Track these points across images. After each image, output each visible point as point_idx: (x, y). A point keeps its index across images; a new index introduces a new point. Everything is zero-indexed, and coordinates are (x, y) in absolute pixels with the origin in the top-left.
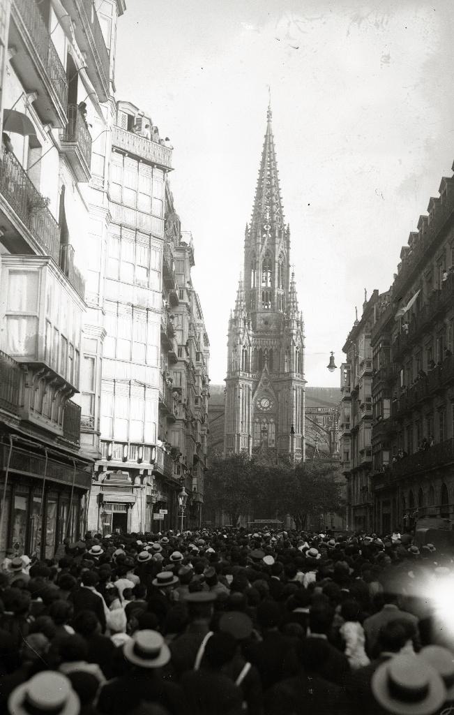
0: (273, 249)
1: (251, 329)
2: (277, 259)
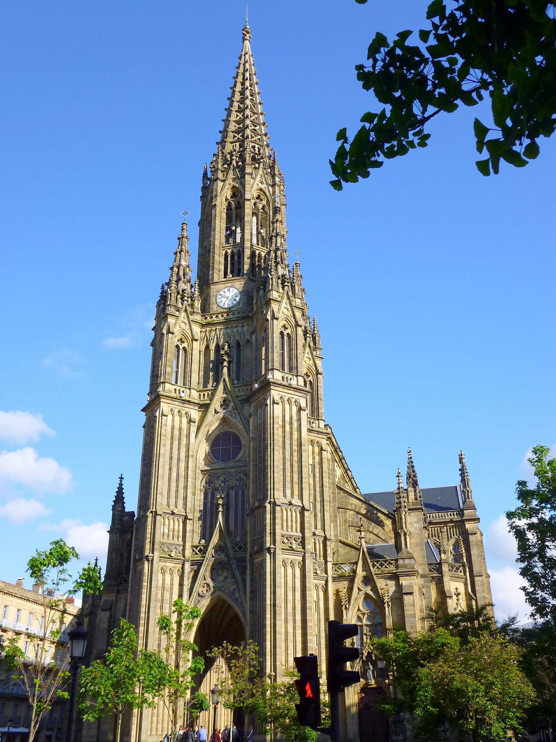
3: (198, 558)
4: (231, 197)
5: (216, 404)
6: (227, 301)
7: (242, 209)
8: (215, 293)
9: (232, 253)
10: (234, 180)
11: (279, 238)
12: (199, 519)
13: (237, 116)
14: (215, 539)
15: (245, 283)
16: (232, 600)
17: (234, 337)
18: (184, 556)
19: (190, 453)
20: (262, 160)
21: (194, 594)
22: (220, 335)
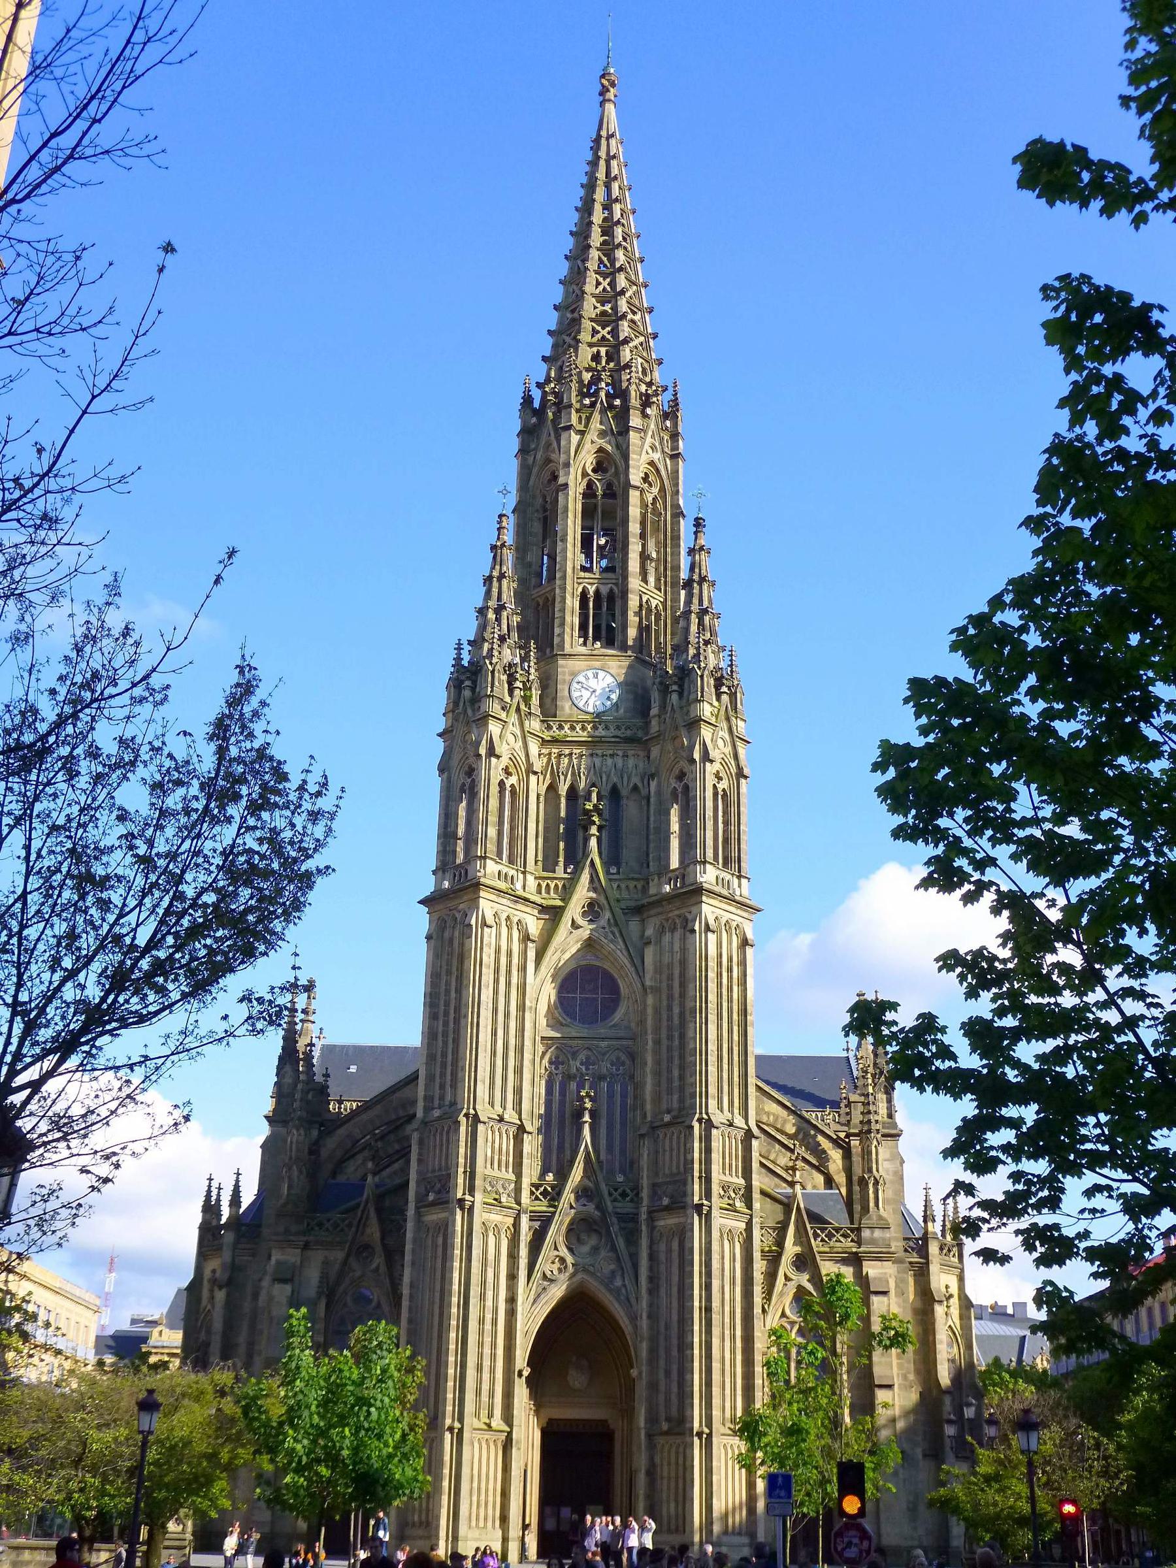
0: (618, 447)
1: (534, 708)
2: (635, 478)
3: (542, 1206)
4: (594, 471)
5: (575, 909)
6: (593, 699)
7: (619, 501)
8: (567, 678)
9: (597, 592)
10: (602, 434)
11: (705, 586)
12: (539, 1131)
13: (598, 284)
14: (577, 1175)
15: (630, 667)
16: (610, 1290)
17: (608, 776)
18: (519, 1203)
19: (528, 1003)
20: (655, 399)
21: (537, 1275)
22: (579, 769)
